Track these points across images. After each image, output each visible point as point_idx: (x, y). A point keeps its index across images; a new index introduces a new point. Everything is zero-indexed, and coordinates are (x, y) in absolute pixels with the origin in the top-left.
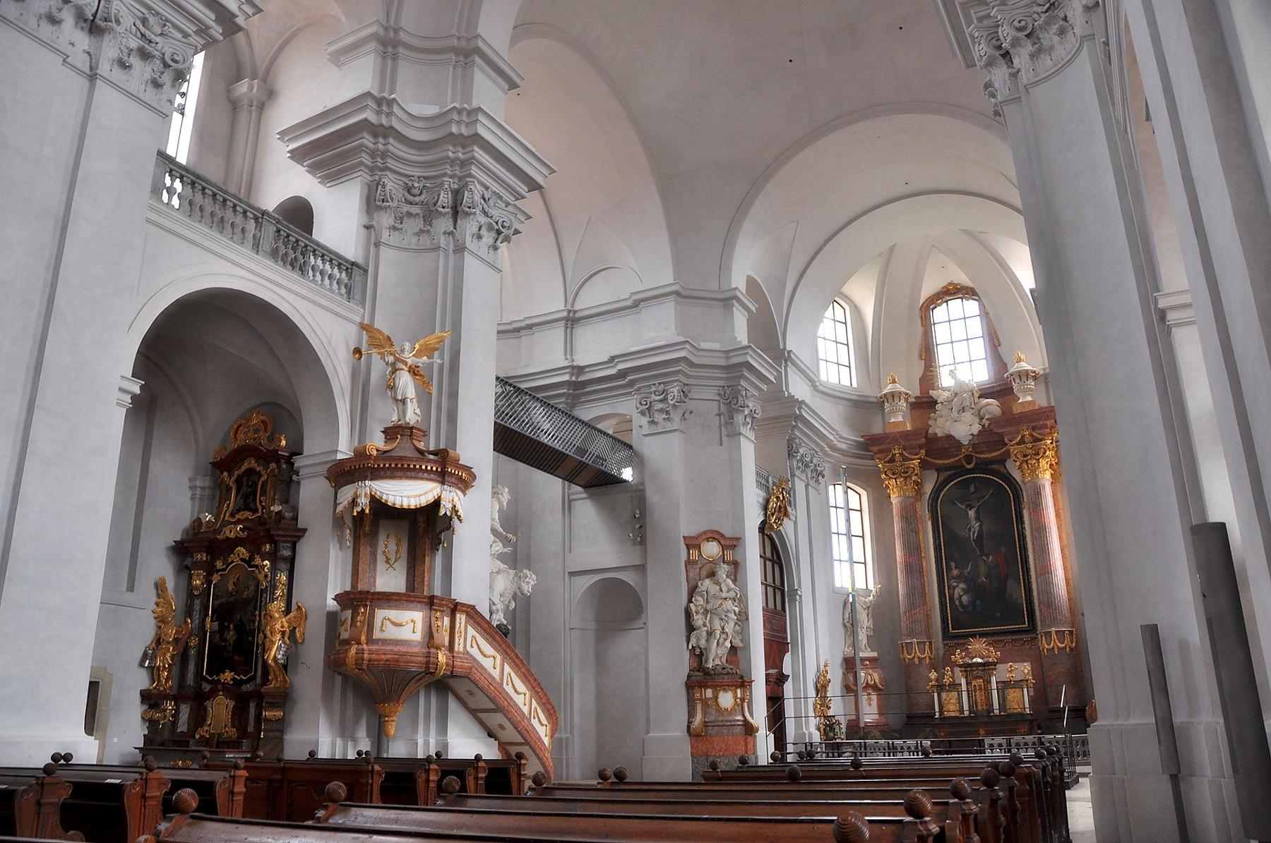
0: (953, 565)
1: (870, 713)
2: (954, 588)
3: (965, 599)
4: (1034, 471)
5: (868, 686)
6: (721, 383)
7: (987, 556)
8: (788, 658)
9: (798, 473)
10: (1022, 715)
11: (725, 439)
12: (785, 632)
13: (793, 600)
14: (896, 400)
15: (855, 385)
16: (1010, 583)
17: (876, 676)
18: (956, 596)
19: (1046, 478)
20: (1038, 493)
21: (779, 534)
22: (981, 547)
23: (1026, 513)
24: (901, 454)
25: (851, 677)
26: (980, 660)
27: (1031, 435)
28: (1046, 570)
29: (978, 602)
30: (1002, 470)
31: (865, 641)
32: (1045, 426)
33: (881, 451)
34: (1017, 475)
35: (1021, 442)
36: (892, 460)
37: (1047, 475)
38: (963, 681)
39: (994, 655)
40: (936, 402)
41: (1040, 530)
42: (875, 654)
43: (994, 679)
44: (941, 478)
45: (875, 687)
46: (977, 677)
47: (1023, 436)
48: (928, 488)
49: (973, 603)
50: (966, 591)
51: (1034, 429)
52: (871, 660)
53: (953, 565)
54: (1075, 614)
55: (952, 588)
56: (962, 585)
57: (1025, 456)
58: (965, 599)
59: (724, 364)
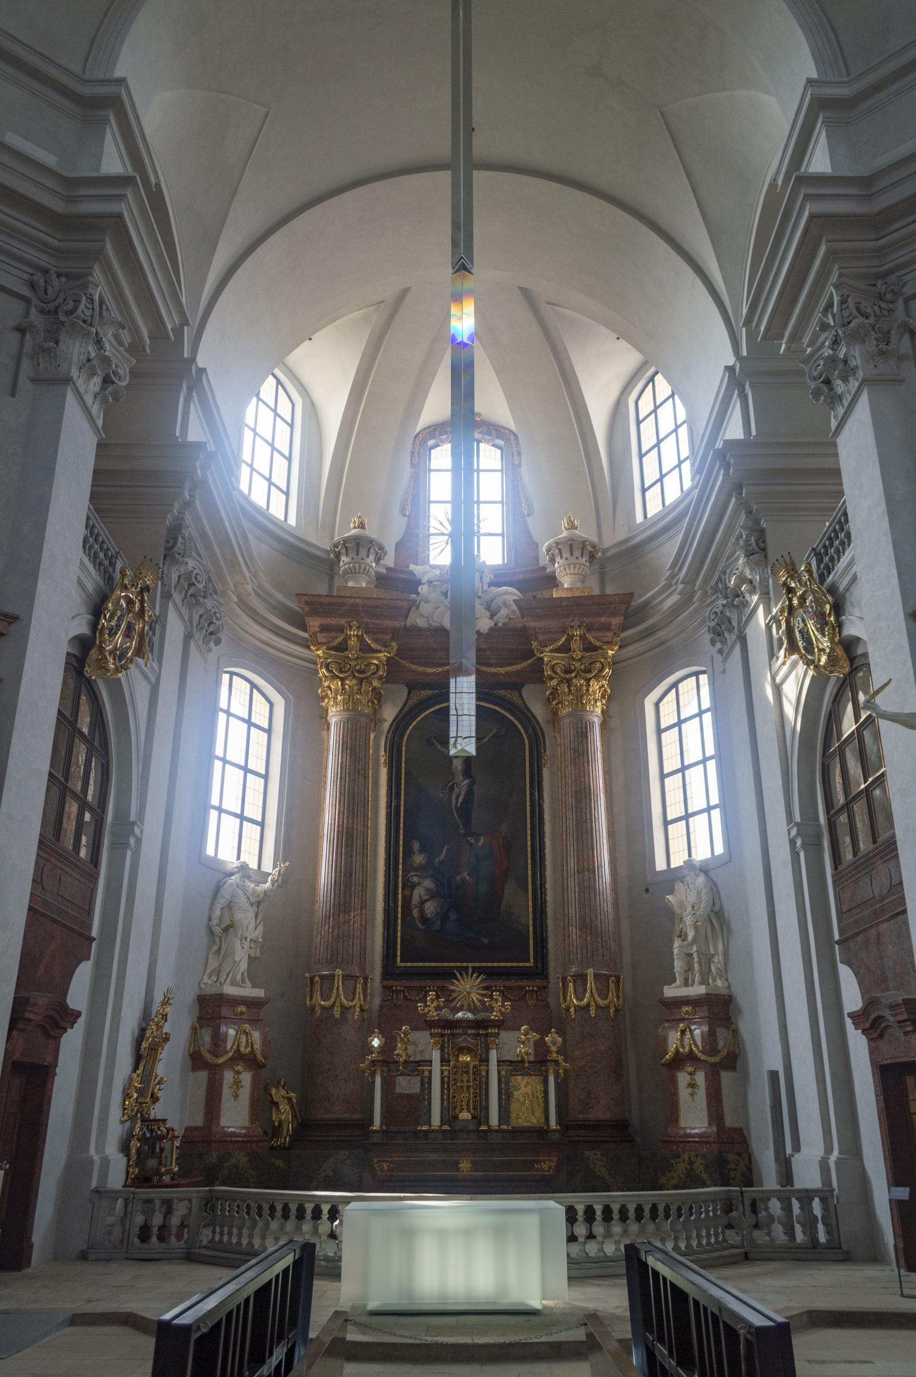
0: (416, 846)
1: (235, 1117)
2: (414, 886)
3: (430, 908)
4: (579, 698)
5: (238, 1057)
6: (44, 260)
7: (477, 836)
8: (83, 977)
9: (177, 597)
10: (541, 1132)
11: (24, 384)
12: (90, 911)
13: (120, 845)
14: (363, 553)
15: (292, 521)
16: (510, 888)
17: (256, 1036)
18: (415, 900)
19: (595, 712)
20: (582, 734)
21: (116, 688)
22: (467, 823)
23: (546, 772)
24: (360, 638)
25: (206, 1036)
26: (470, 1016)
27: (583, 638)
28: (587, 868)
29: (453, 916)
30: (516, 700)
31: (244, 966)
32: (607, 627)
33: (324, 629)
34: (539, 711)
35: (565, 648)
36: (342, 647)
37: (598, 711)
38: (436, 1056)
39: (499, 1007)
40: (419, 583)
41: (582, 795)
42: (260, 993)
43: (493, 1056)
44: (414, 700)
45: (251, 1061)
46: (462, 1050)
47: (570, 638)
48: (389, 713)
49: (444, 917)
50: (433, 895)
51: (590, 628)
52: (253, 1004)
53: (416, 846)
54: (717, 919)
55: (409, 886)
56: (428, 883)
57: (568, 671)
58: (430, 908)
59: (57, 206)
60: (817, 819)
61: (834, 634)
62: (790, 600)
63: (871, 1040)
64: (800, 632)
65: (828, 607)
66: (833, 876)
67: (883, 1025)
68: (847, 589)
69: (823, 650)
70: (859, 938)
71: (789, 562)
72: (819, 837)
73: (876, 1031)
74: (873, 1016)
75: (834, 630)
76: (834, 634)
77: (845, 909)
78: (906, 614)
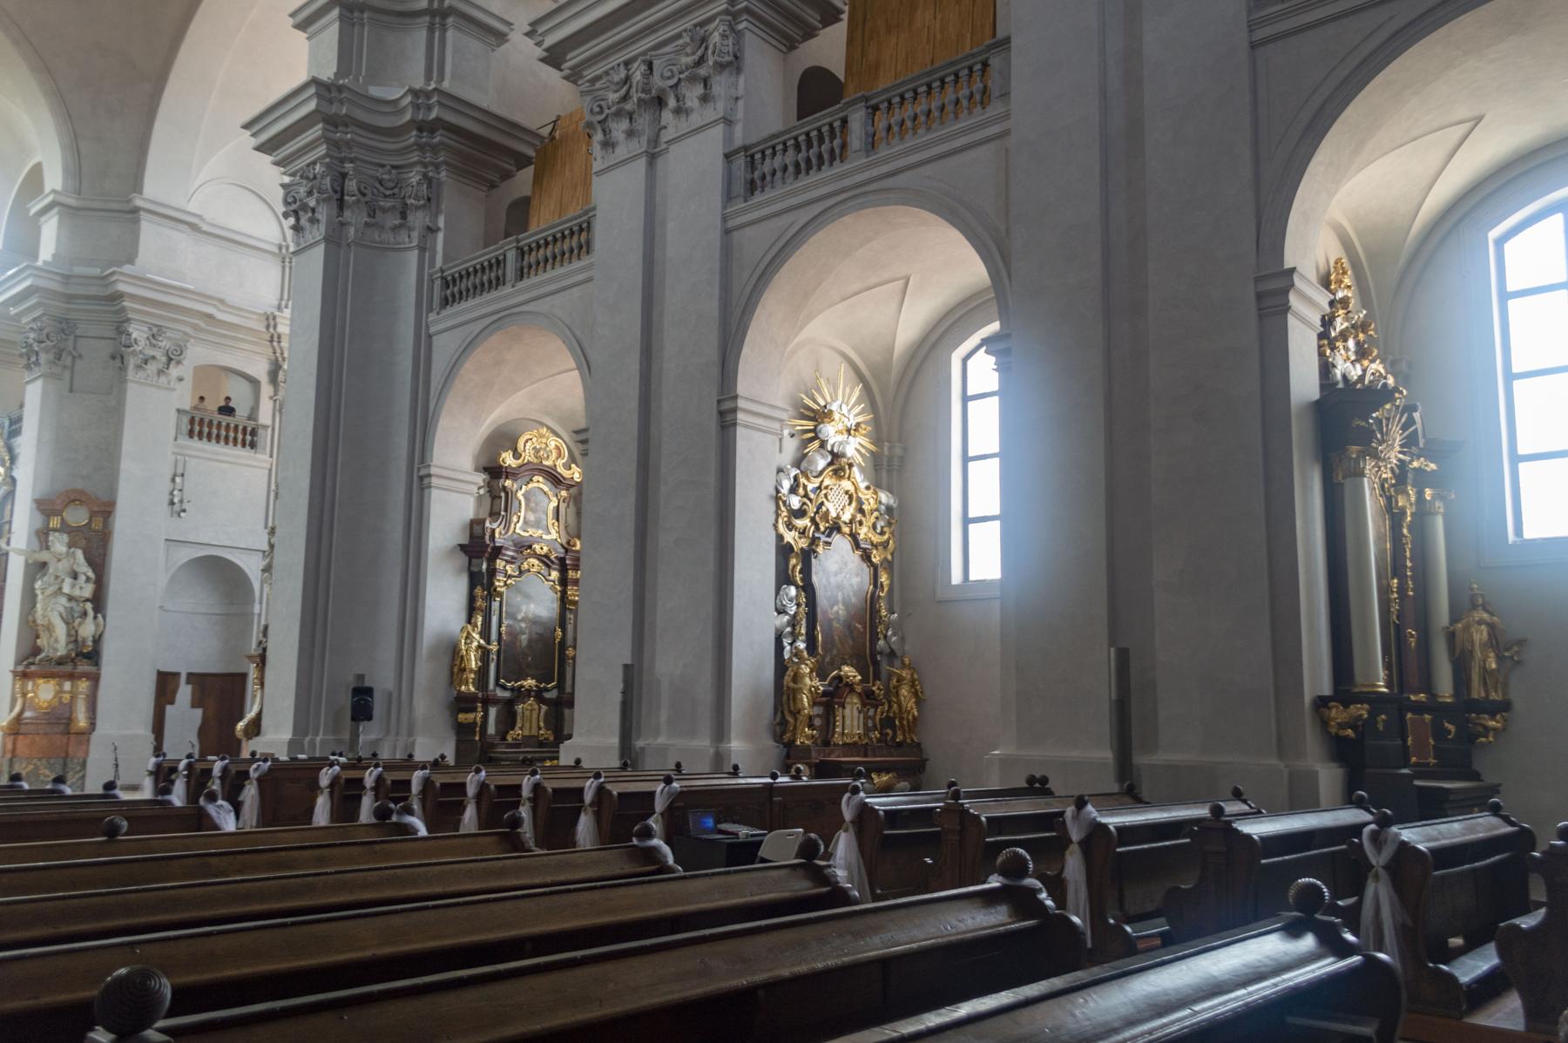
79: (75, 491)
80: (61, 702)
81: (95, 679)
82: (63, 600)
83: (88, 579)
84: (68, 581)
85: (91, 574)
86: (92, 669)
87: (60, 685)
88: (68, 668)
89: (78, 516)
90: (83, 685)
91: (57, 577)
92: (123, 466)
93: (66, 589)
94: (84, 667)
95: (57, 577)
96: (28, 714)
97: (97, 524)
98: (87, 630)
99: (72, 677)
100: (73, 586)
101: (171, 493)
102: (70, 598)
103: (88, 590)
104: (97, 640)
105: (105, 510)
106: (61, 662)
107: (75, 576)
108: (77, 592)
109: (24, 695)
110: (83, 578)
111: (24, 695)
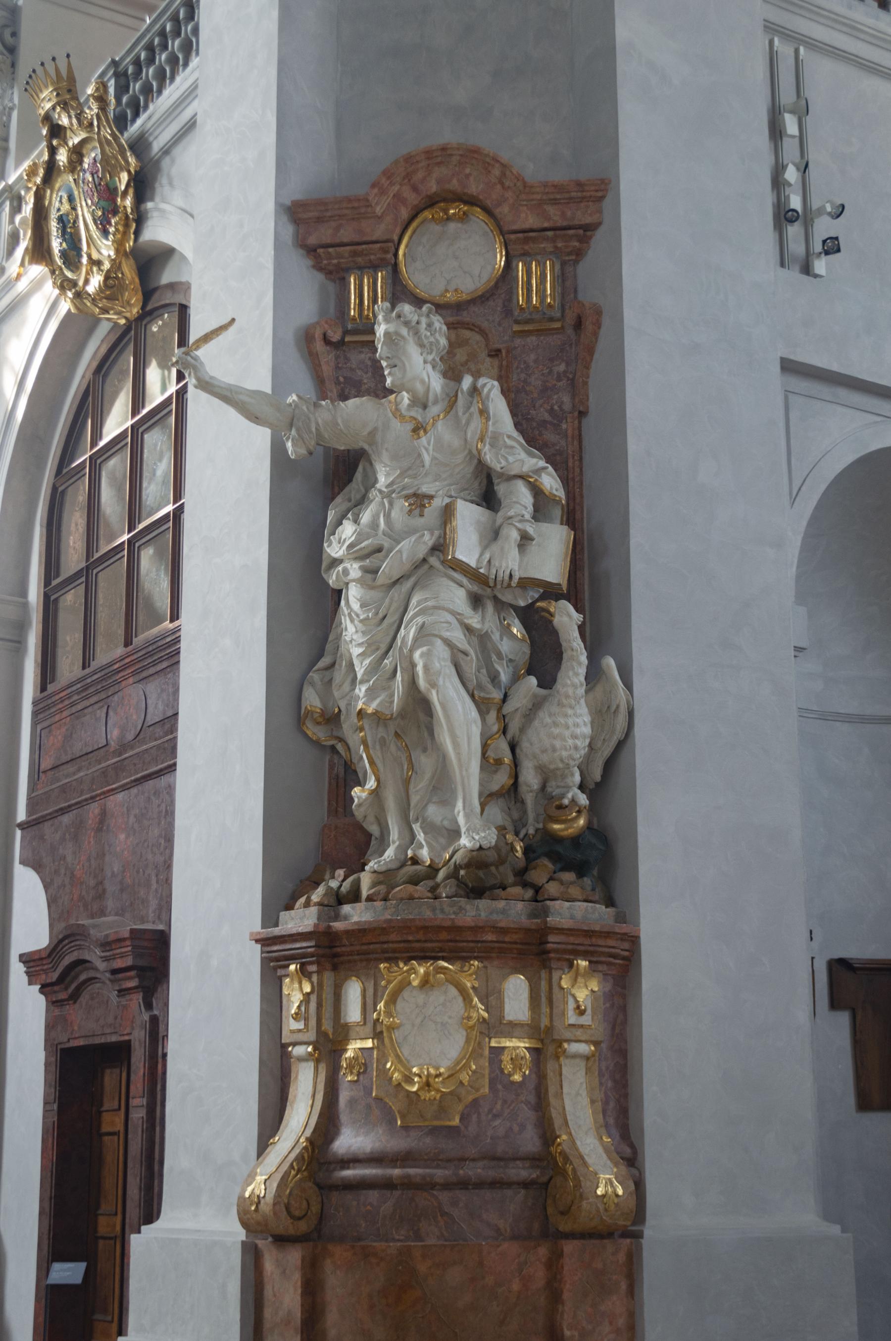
60: (24, 593)
61: (125, 233)
62: (53, 151)
63: (53, 1003)
64: (61, 219)
65: (125, 177)
66: (35, 703)
67: (83, 977)
68: (166, 151)
69: (98, 263)
70: (66, 819)
71: (64, 72)
72: (21, 627)
73: (66, 989)
74: (67, 961)
75: (127, 226)
76: (125, 233)
77: (46, 764)
78: (279, 205)
79: (438, 156)
80: (498, 1078)
81: (619, 960)
82: (455, 596)
83: (542, 504)
84: (468, 517)
85: (550, 482)
86: (597, 914)
87: (492, 997)
88: (511, 910)
89: (460, 258)
90: (582, 990)
91: (419, 501)
92: (622, 33)
93: (467, 549)
94: (572, 910)
95: (419, 501)
96: (350, 1140)
97: (536, 284)
98: (568, 728)
99: (536, 951)
100: (492, 535)
101: (778, 182)
102: (484, 589)
103: (549, 556)
104: (609, 772)
105: (569, 221)
106: (478, 877)
107: (488, 499)
108: (510, 562)
109: (329, 1047)
110: (524, 497)
111: (329, 1047)
